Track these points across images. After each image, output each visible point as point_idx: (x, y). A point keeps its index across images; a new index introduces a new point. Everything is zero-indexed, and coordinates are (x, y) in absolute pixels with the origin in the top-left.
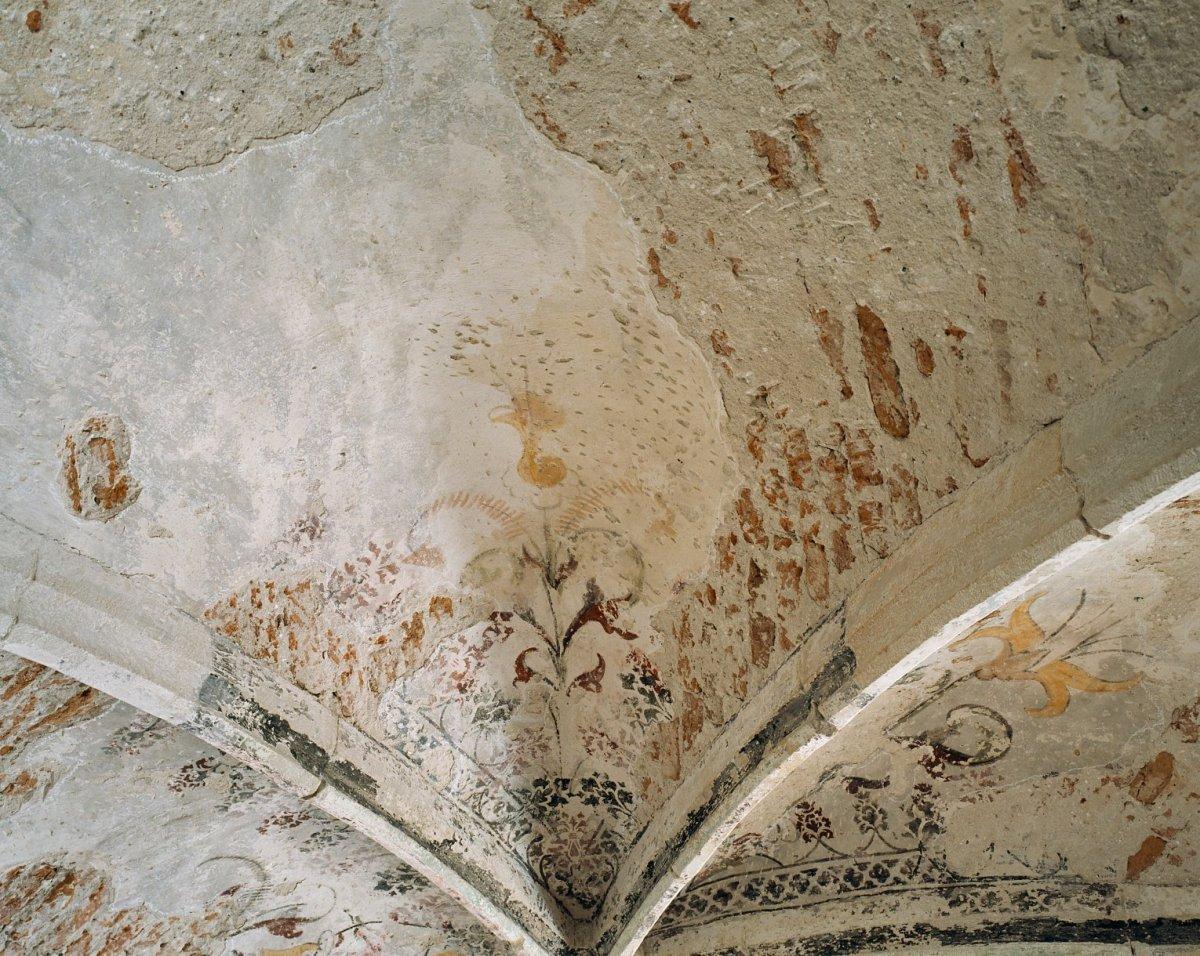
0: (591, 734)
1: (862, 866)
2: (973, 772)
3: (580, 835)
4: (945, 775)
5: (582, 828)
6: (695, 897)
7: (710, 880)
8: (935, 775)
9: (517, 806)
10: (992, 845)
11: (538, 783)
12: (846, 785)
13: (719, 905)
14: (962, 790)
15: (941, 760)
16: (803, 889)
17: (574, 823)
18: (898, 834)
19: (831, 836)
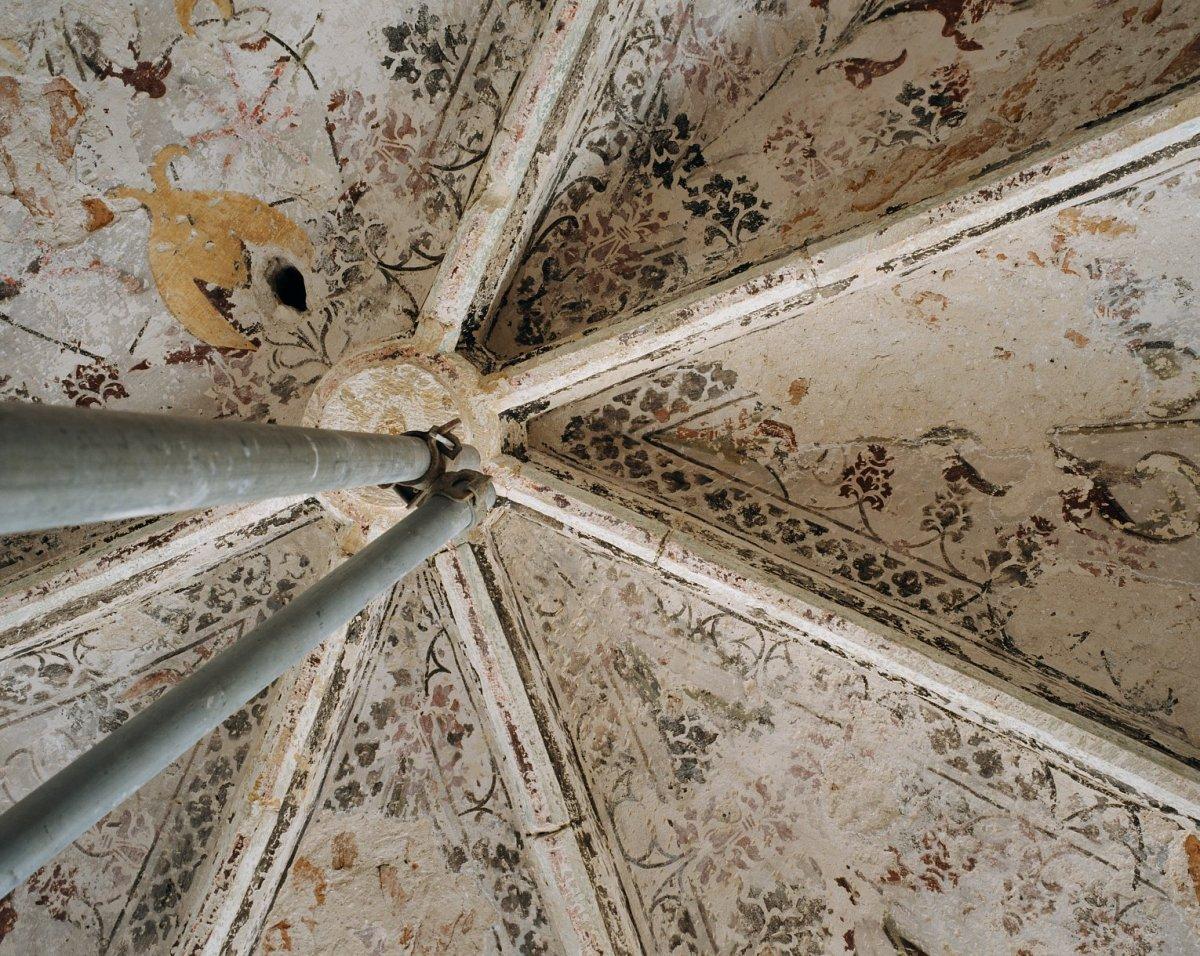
0: (794, 128)
1: (890, 563)
2: (1121, 540)
3: (634, 238)
4: (1083, 525)
5: (647, 231)
6: (643, 455)
7: (682, 450)
8: (1069, 517)
9: (640, 116)
10: (1086, 634)
11: (682, 122)
12: (949, 465)
13: (663, 486)
14: (1091, 553)
15: (1092, 505)
16: (790, 539)
17: (645, 217)
18: (970, 554)
19: (879, 508)
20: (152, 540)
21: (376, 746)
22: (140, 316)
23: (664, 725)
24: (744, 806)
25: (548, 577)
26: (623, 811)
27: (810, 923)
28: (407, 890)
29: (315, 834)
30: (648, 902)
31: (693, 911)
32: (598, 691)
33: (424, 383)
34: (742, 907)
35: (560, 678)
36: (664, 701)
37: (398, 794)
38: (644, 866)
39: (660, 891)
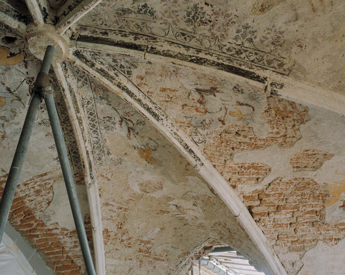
20: (63, 90)
21: (121, 65)
22: (15, 70)
23: (139, 12)
24: (165, 6)
25: (93, 19)
26: (154, 31)
27: (198, 10)
28: (152, 71)
29: (134, 81)
30: (175, 38)
31: (181, 31)
32: (125, 22)
33: (33, 40)
34: (186, 22)
35: (119, 28)
36: (133, 9)
37: (133, 65)
38: (167, 35)
39: (174, 35)
